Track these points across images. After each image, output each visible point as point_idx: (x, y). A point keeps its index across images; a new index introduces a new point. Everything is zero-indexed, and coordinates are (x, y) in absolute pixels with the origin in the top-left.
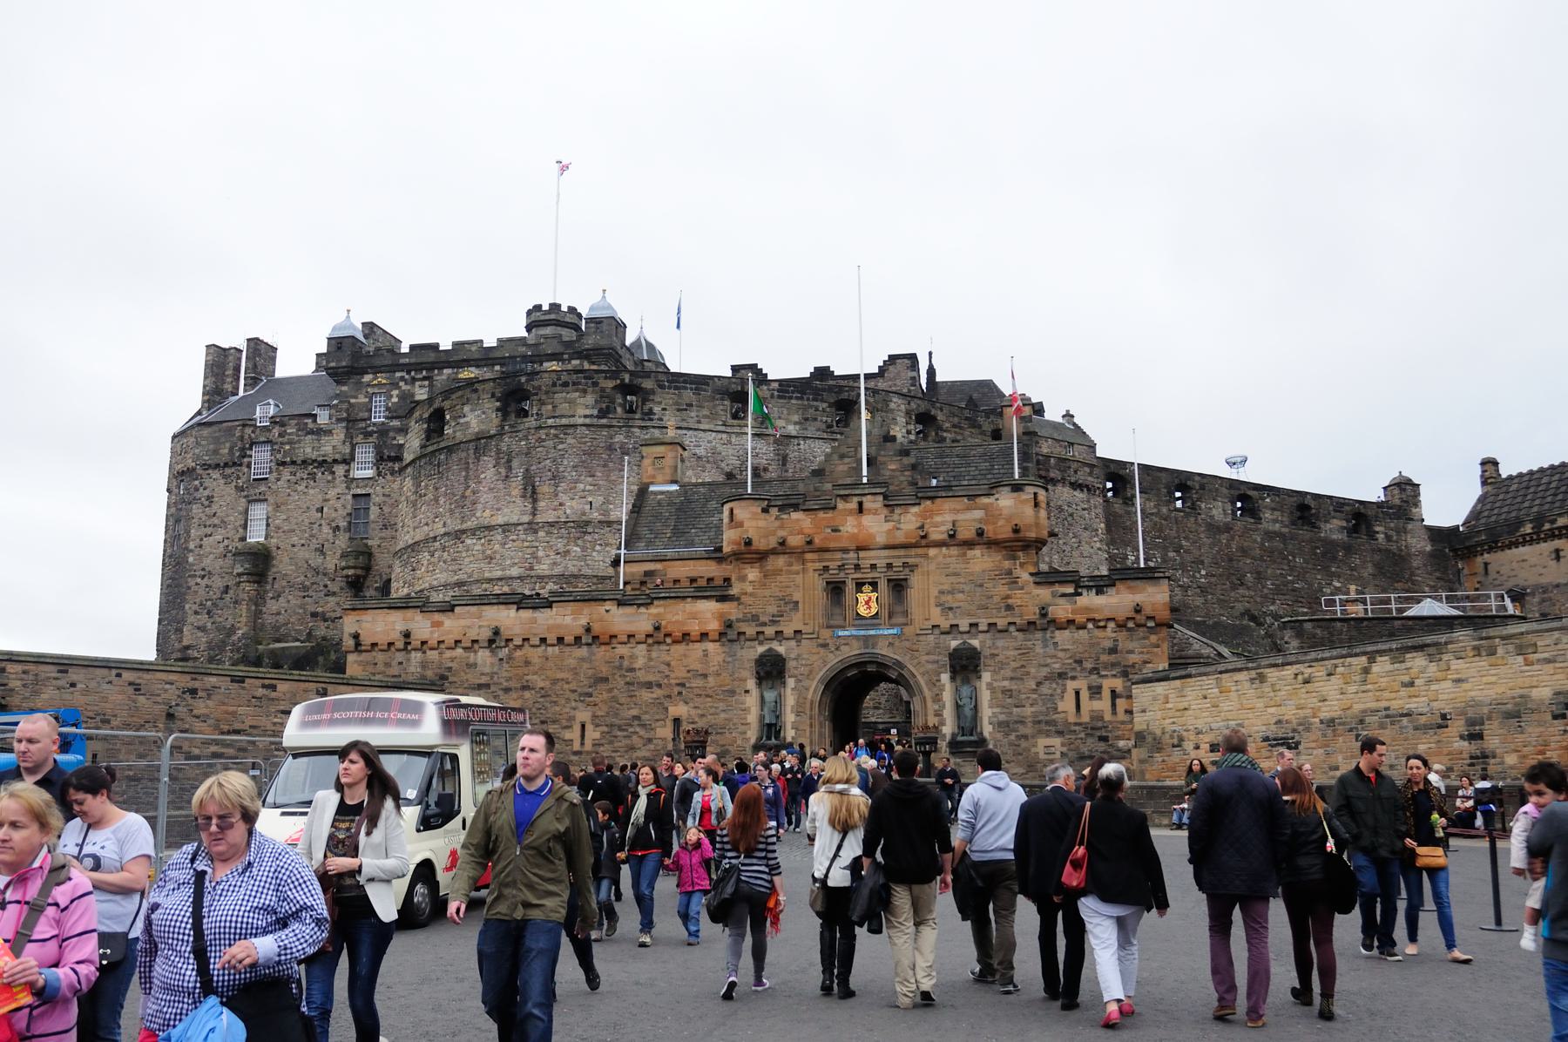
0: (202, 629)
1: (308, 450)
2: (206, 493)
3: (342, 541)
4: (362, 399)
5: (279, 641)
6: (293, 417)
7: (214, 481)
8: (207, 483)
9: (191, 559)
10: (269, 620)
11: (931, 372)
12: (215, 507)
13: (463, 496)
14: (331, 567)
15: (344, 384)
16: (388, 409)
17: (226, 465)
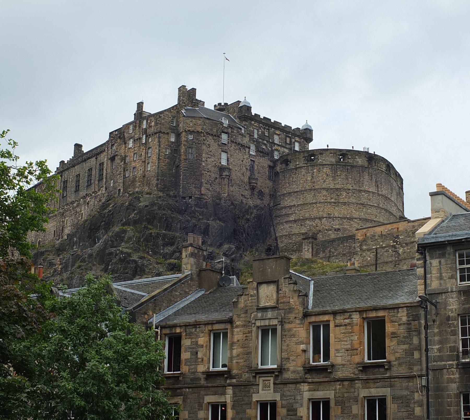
2: (208, 143)
3: (248, 173)
7: (210, 140)
8: (208, 139)
12: (211, 149)
13: (359, 181)
15: (247, 122)
17: (215, 135)
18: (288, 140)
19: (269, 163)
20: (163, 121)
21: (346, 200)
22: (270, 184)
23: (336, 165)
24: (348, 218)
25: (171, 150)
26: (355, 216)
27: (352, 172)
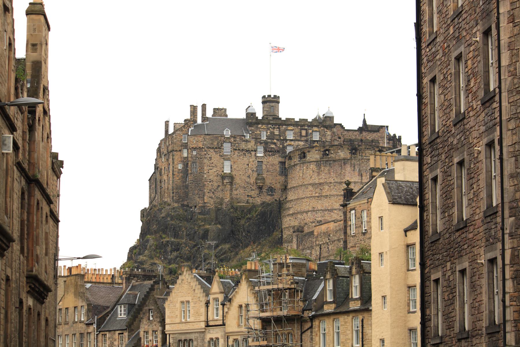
0: (211, 198)
1: (244, 146)
2: (209, 156)
3: (255, 175)
4: (258, 132)
5: (238, 203)
6: (238, 136)
8: (209, 153)
9: (205, 176)
10: (234, 196)
11: (364, 121)
12: (212, 161)
14: (252, 182)
15: (252, 127)
16: (266, 136)
17: (216, 148)
18: (304, 133)
19: (281, 159)
20: (175, 140)
21: (328, 193)
22: (283, 178)
23: (320, 161)
24: (328, 210)
25: (184, 165)
26: (335, 207)
27: (334, 166)
